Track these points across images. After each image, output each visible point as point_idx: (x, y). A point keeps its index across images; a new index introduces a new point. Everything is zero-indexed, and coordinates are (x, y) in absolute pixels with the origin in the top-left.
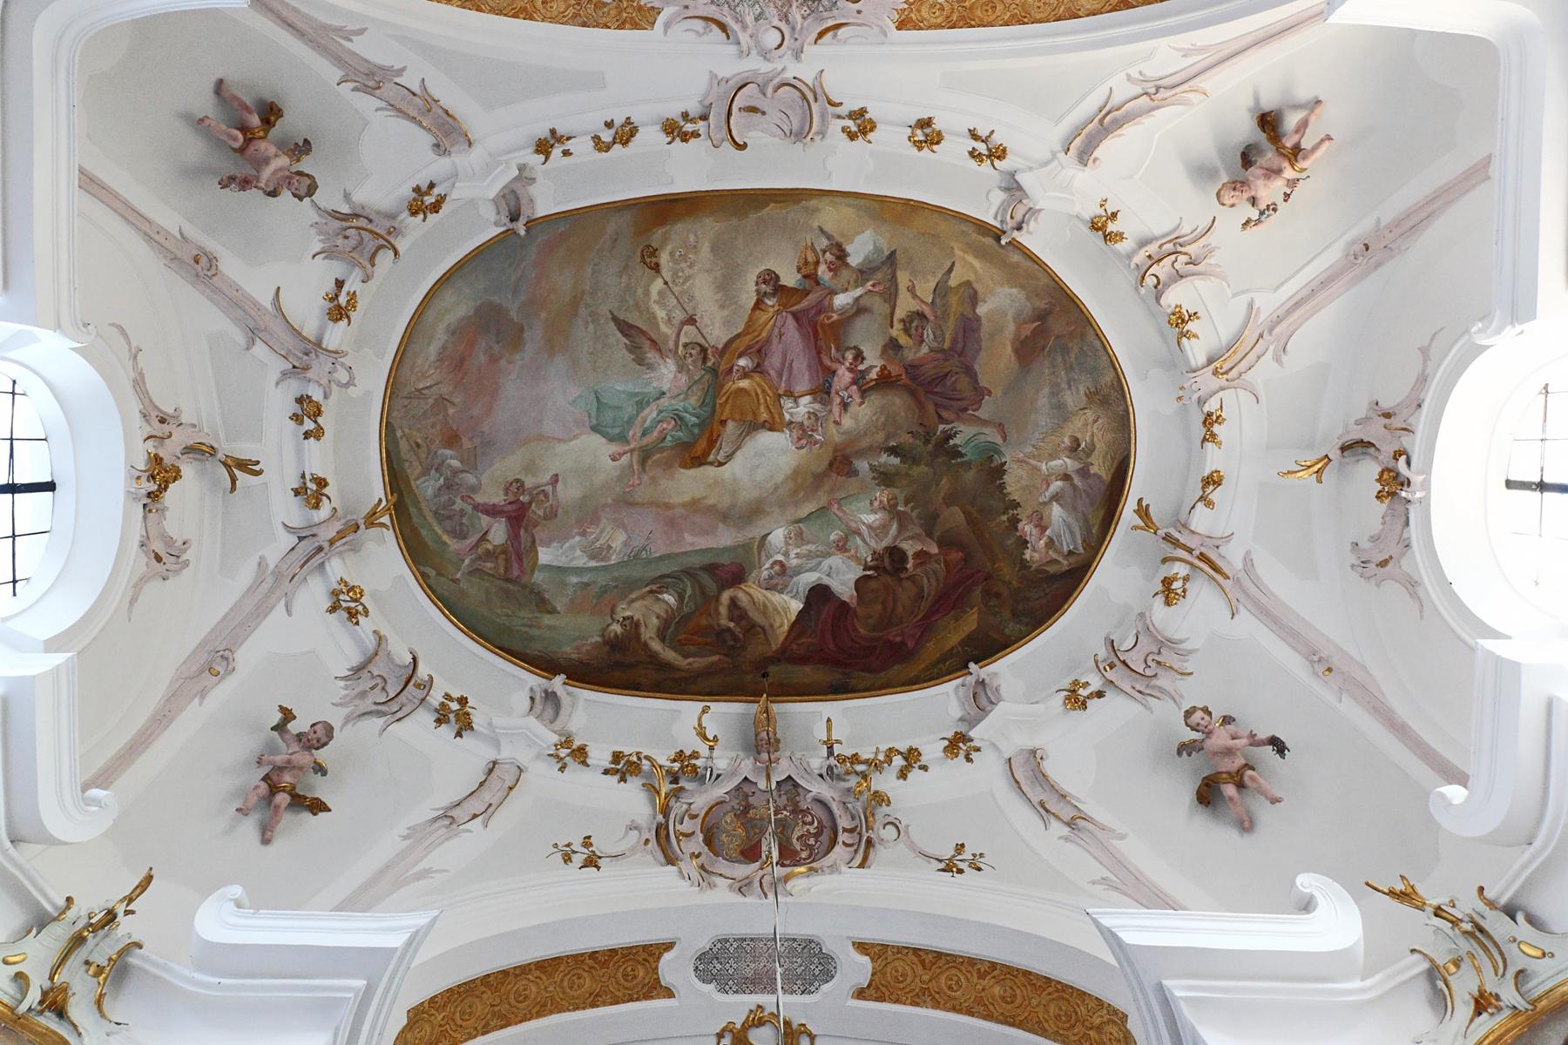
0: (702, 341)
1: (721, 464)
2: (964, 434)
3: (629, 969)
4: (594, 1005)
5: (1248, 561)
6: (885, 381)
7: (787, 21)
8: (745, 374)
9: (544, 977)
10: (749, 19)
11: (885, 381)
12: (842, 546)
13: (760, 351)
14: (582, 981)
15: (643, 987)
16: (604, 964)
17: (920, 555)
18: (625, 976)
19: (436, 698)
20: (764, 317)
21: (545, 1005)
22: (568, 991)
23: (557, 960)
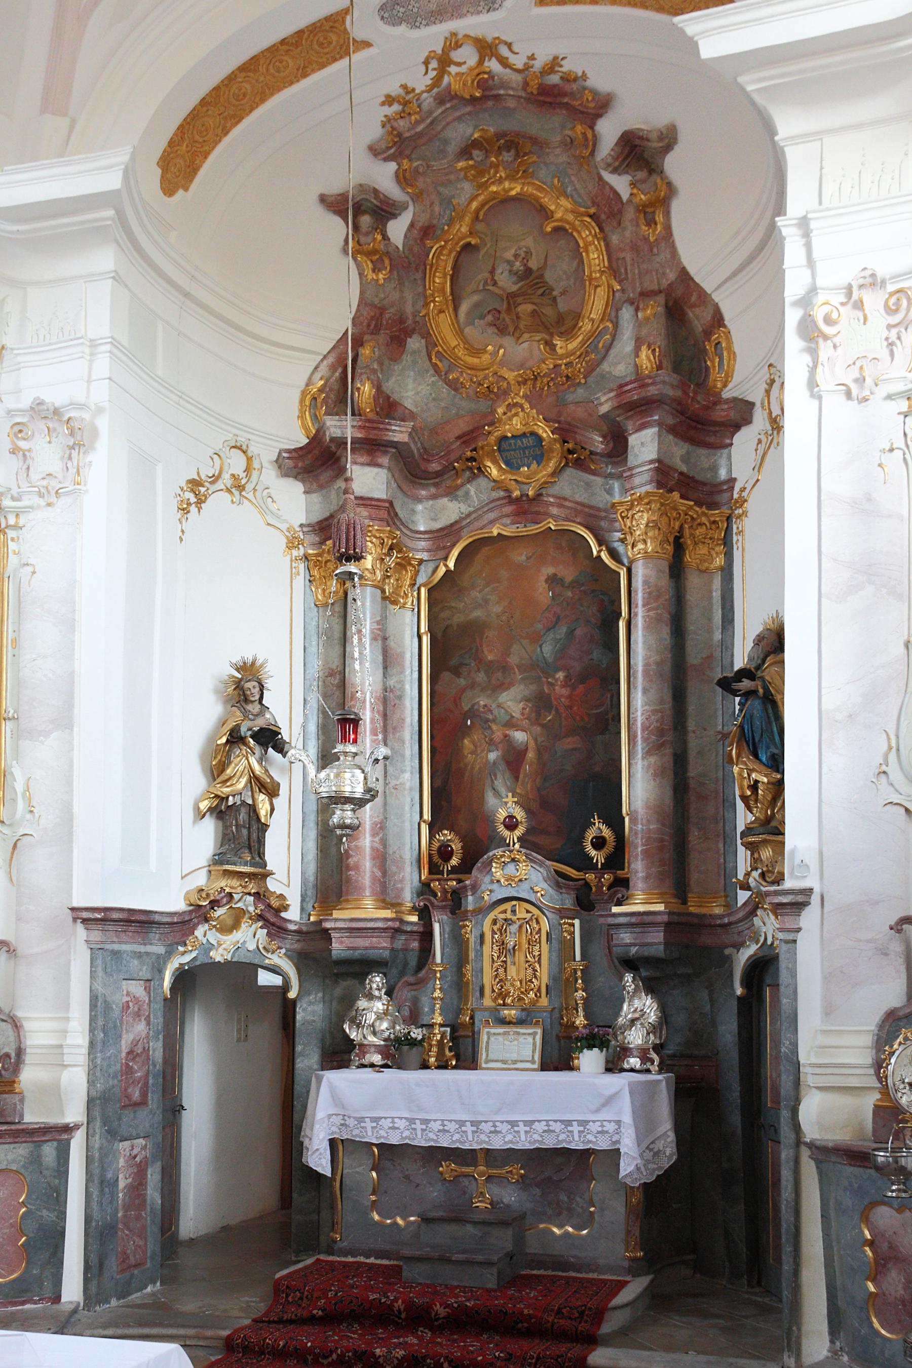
3: (322, 39)
4: (305, 75)
9: (251, 74)
14: (284, 63)
15: (341, 49)
16: (297, 45)
18: (321, 45)
21: (263, 93)
22: (277, 74)
23: (255, 59)
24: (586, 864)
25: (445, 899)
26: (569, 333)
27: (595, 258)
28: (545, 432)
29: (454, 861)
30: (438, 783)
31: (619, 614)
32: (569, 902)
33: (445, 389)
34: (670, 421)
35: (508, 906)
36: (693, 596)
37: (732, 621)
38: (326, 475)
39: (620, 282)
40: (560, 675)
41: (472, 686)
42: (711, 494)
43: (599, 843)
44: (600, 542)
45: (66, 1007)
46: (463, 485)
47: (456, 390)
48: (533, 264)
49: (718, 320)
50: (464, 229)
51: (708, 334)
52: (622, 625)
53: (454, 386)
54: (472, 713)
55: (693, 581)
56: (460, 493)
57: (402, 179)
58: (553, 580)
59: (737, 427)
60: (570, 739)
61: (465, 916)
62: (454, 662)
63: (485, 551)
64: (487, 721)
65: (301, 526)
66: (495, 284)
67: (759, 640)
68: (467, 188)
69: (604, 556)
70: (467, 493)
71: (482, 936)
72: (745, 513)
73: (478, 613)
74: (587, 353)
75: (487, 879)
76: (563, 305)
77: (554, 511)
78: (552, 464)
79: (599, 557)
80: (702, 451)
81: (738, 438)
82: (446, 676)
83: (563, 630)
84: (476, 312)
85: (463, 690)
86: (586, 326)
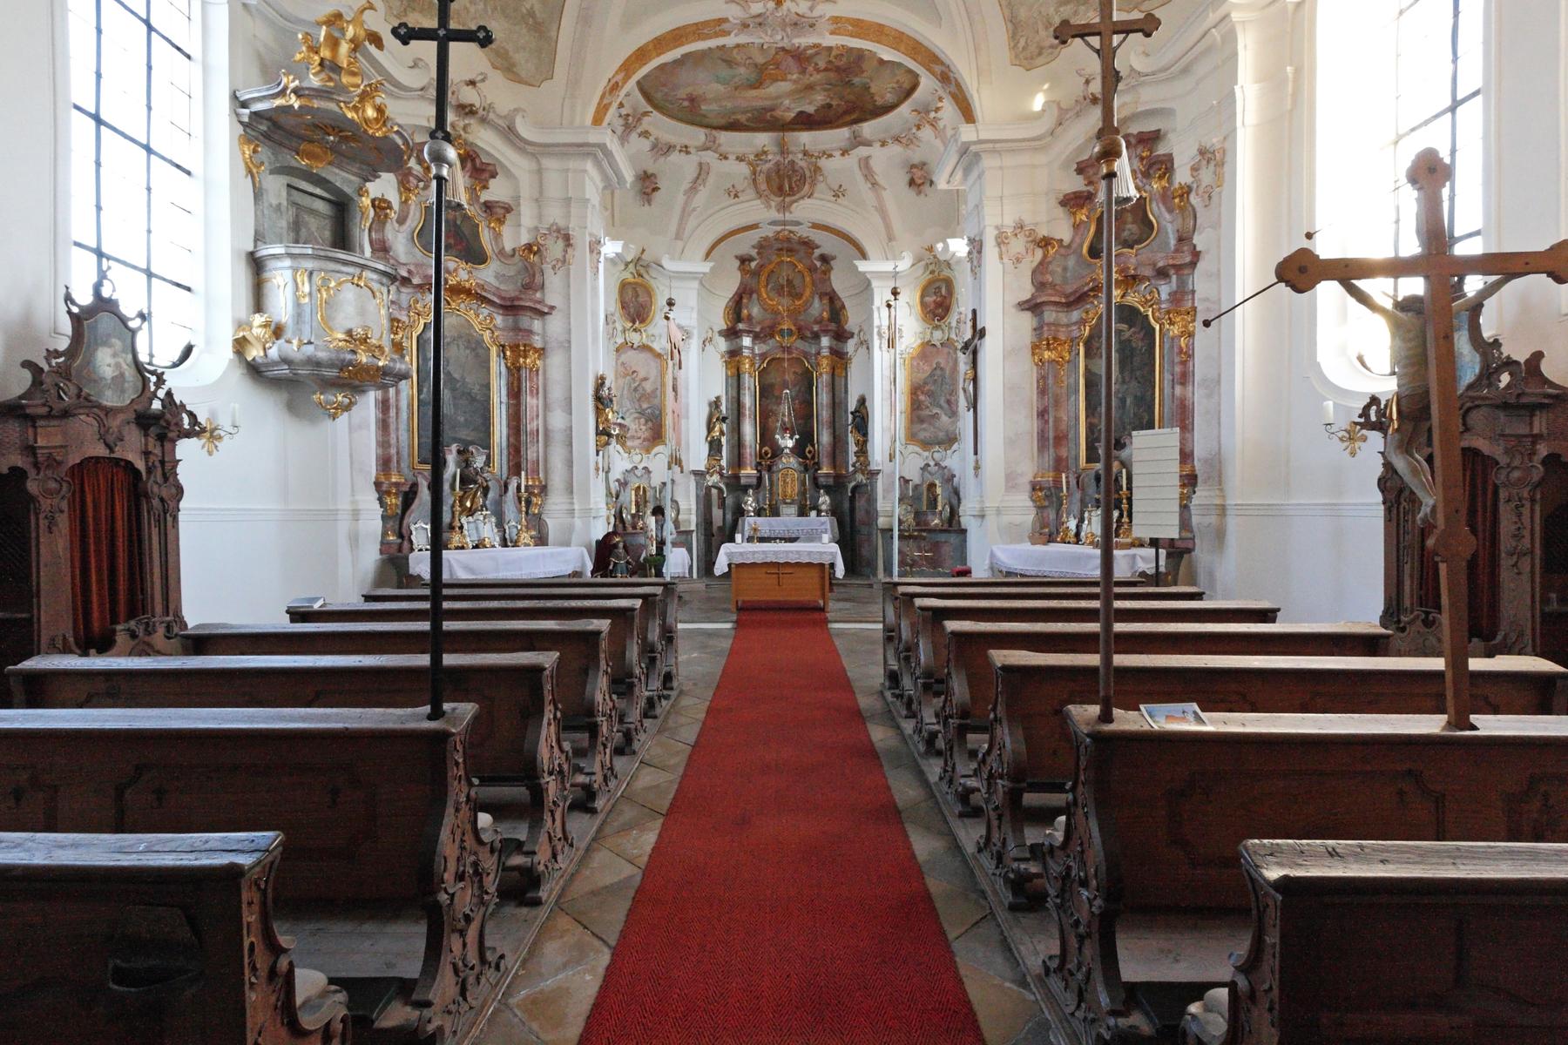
2: (856, 80)
5: (945, 127)
6: (826, 70)
10: (769, 32)
11: (826, 70)
12: (810, 103)
17: (838, 105)
26: (800, 298)
27: (808, 279)
28: (793, 328)
36: (836, 383)
53: (765, 310)
54: (771, 411)
55: (836, 378)
57: (758, 253)
58: (795, 373)
67: (858, 401)
68: (775, 257)
83: (797, 388)
84: (773, 289)
86: (804, 298)
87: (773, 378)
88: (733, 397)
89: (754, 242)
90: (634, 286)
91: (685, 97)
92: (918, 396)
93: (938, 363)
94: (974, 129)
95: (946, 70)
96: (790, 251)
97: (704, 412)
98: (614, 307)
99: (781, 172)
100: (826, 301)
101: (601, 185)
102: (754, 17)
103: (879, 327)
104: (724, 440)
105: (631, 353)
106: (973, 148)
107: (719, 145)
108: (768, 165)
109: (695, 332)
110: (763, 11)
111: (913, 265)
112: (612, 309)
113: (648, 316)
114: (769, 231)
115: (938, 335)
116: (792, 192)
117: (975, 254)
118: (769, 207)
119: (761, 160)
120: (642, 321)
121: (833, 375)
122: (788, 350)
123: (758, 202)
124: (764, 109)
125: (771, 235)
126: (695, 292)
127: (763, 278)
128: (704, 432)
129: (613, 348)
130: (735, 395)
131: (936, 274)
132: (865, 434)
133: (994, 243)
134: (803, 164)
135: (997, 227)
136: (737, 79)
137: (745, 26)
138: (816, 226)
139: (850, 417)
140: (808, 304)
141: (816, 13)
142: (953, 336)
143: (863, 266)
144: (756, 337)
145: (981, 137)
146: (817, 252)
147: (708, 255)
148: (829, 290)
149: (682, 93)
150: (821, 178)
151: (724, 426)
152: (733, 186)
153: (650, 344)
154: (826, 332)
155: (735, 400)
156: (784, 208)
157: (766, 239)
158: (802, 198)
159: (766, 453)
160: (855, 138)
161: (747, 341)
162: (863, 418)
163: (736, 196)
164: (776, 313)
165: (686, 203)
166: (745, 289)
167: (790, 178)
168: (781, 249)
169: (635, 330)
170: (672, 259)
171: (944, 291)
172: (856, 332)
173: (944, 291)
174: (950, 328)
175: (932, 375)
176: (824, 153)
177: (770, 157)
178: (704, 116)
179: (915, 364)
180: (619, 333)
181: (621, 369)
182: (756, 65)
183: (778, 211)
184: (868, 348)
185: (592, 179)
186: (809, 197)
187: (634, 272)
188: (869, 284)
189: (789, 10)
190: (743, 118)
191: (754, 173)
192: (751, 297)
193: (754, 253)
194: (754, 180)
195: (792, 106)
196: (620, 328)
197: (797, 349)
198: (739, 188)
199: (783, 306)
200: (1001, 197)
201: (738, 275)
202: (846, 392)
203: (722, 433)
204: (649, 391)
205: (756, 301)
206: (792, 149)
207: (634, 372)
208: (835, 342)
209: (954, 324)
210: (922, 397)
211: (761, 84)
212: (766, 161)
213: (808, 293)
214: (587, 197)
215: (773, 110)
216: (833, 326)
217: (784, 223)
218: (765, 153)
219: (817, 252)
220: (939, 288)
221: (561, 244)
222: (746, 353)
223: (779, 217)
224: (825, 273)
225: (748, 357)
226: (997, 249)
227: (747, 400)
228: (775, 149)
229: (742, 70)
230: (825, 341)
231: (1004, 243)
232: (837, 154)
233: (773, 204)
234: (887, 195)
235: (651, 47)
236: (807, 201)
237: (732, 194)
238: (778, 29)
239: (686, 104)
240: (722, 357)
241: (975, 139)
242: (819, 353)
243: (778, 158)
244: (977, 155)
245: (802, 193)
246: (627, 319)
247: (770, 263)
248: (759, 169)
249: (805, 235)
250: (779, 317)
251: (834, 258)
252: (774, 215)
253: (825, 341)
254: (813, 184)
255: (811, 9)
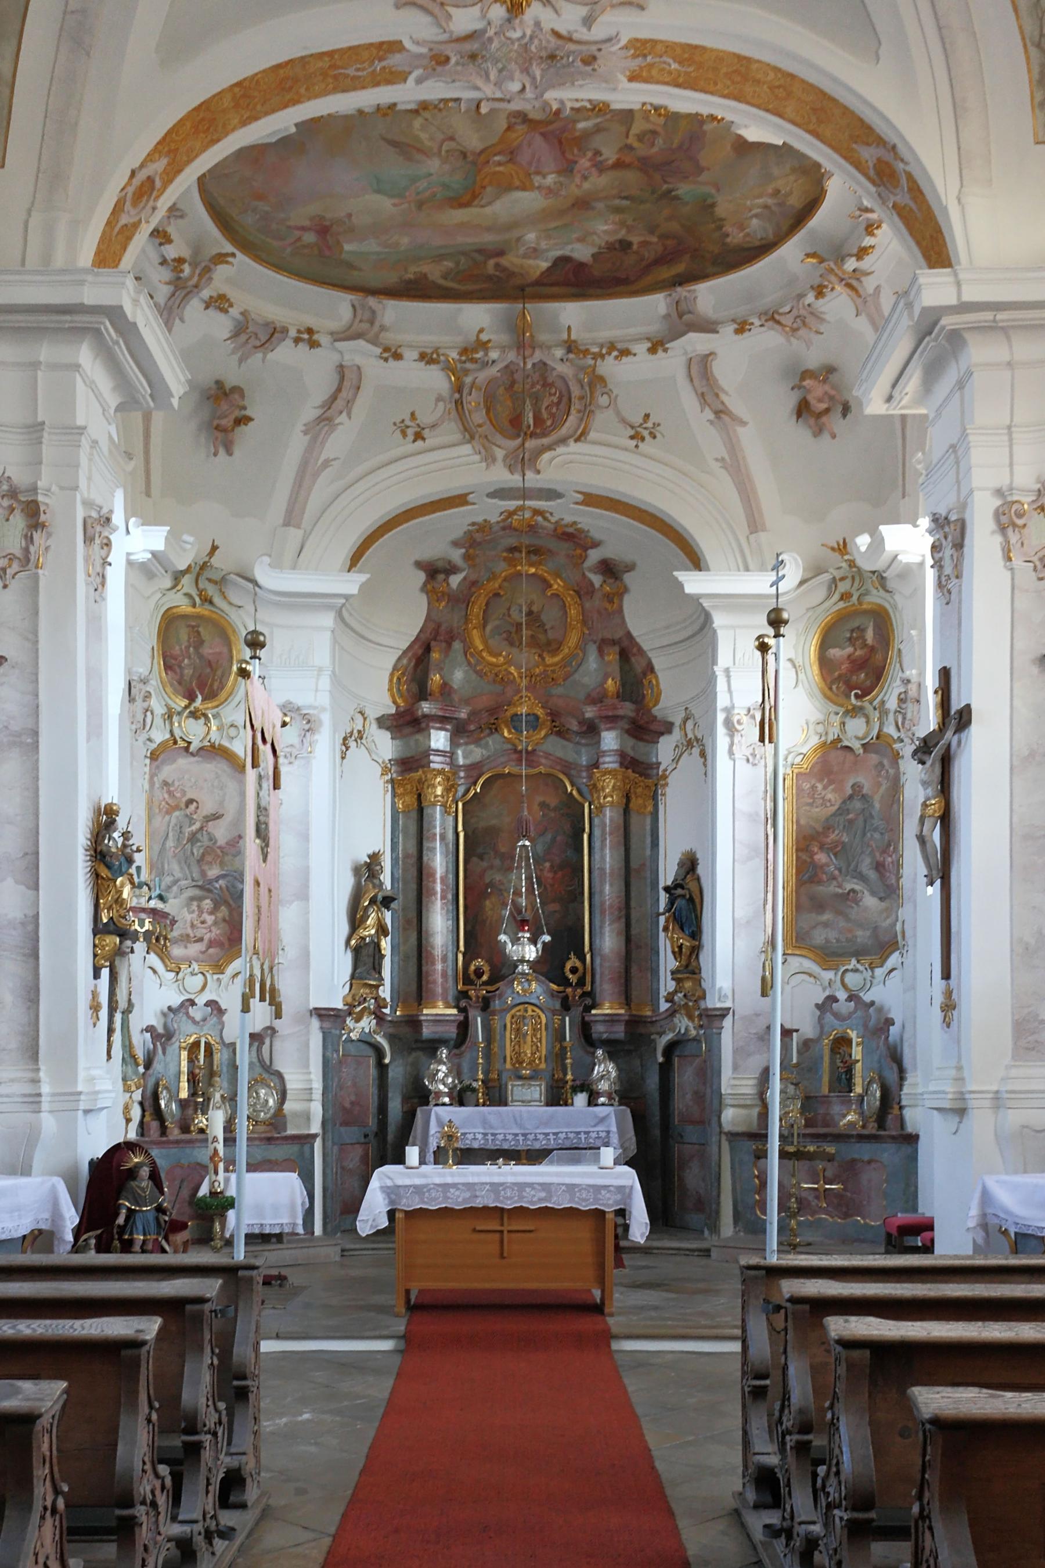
0: (459, 147)
1: (482, 206)
6: (619, 165)
7: (528, 73)
8: (500, 164)
11: (619, 165)
13: (512, 155)
19: (293, 333)
20: (514, 135)
24: (566, 983)
25: (477, 1002)
26: (555, 652)
28: (540, 712)
29: (485, 978)
30: (469, 928)
31: (584, 830)
32: (558, 1005)
33: (474, 676)
34: (627, 726)
35: (521, 1007)
36: (634, 828)
37: (658, 845)
38: (407, 730)
39: (588, 629)
40: (547, 865)
41: (491, 867)
42: (646, 769)
43: (574, 970)
44: (572, 784)
45: (307, 1066)
46: (484, 737)
47: (481, 677)
48: (535, 608)
49: (650, 668)
50: (497, 585)
51: (645, 674)
52: (586, 837)
53: (480, 674)
54: (491, 884)
55: (634, 819)
56: (483, 742)
57: (467, 557)
58: (543, 805)
59: (662, 734)
60: (553, 905)
61: (493, 1013)
62: (480, 850)
63: (500, 782)
64: (501, 890)
65: (390, 760)
66: (509, 616)
67: (681, 864)
68: (503, 565)
69: (575, 793)
70: (487, 743)
71: (505, 1026)
72: (667, 784)
73: (494, 822)
74: (565, 667)
75: (509, 991)
76: (551, 635)
77: (543, 761)
78: (543, 733)
79: (571, 793)
80: (641, 744)
81: (662, 739)
82: (475, 859)
83: (549, 836)
85: (485, 871)
87: (495, 816)
88: (406, 856)
89: (458, 533)
90: (194, 624)
91: (307, 223)
92: (812, 855)
93: (857, 787)
94: (951, 279)
95: (889, 157)
96: (535, 551)
97: (346, 884)
98: (148, 664)
99: (518, 387)
100: (612, 656)
101: (113, 401)
102: (459, 39)
103: (728, 710)
104: (386, 944)
105: (183, 762)
106: (948, 322)
107: (383, 328)
108: (493, 371)
109: (326, 718)
110: (479, 25)
111: (802, 583)
112: (143, 670)
113: (222, 687)
114: (492, 511)
115: (856, 727)
116: (541, 428)
117: (948, 552)
118: (490, 459)
119: (474, 361)
120: (211, 695)
121: (626, 811)
122: (530, 757)
123: (467, 449)
124: (480, 251)
125: (494, 518)
126: (328, 635)
127: (477, 610)
128: (344, 928)
129: (143, 750)
130: (412, 850)
131: (855, 598)
132: (696, 934)
133: (992, 525)
134: (564, 369)
135: (999, 492)
136: (422, 185)
137: (440, 60)
138: (591, 500)
139: (663, 898)
140: (573, 664)
141: (598, 32)
142: (890, 730)
143: (693, 583)
144: (459, 732)
145: (966, 297)
146: (594, 556)
147: (355, 560)
148: (619, 634)
149: (301, 215)
150: (603, 400)
151: (388, 916)
152: (413, 414)
153: (226, 743)
154: (612, 720)
155: (413, 860)
156: (522, 462)
157: (483, 527)
158: (563, 441)
159: (479, 973)
160: (680, 316)
161: (439, 739)
162: (691, 900)
163: (419, 436)
164: (503, 680)
165: (310, 449)
166: (436, 634)
167: (537, 400)
168: (513, 549)
169: (194, 715)
170: (277, 565)
171: (870, 635)
172: (678, 721)
173: (870, 635)
174: (884, 712)
175: (842, 811)
176: (612, 347)
177: (494, 355)
178: (351, 266)
179: (806, 786)
180: (159, 721)
181: (161, 795)
182: (464, 155)
183: (511, 469)
184: (703, 754)
185: (91, 385)
186: (577, 440)
187: (194, 593)
188: (707, 619)
189: (537, 24)
190: (434, 272)
191: (459, 388)
192: (449, 645)
193: (456, 555)
194: (459, 404)
195: (543, 245)
196: (159, 710)
197: (547, 755)
198: (425, 418)
199: (519, 667)
200: (1009, 427)
201: (423, 601)
202: (655, 844)
203: (382, 930)
204: (221, 842)
205: (461, 658)
206: (543, 337)
207: (190, 801)
208: (631, 742)
209: (892, 704)
210: (821, 857)
211: (474, 197)
212: (486, 364)
213: (573, 639)
214: (80, 422)
215: (501, 253)
216: (627, 709)
217: (524, 493)
218: (484, 346)
219: (594, 556)
220: (861, 630)
221: (19, 521)
222: (437, 763)
223: (514, 480)
224: (609, 598)
225: (441, 772)
226: (998, 539)
227: (438, 862)
228: (504, 338)
229: (434, 165)
230: (610, 740)
231: (1014, 525)
232: (641, 348)
233: (500, 453)
234: (746, 436)
235: (227, 102)
236: (573, 447)
237: (410, 432)
238: (513, 66)
239: (310, 238)
240: (385, 771)
241: (953, 301)
242: (596, 765)
243: (512, 356)
244: (956, 339)
245: (564, 431)
246: (176, 692)
247: (493, 577)
248: (468, 380)
249: (568, 519)
250: (509, 691)
251: (631, 567)
252: (501, 476)
253: (610, 740)
254: (587, 412)
255: (588, 21)
